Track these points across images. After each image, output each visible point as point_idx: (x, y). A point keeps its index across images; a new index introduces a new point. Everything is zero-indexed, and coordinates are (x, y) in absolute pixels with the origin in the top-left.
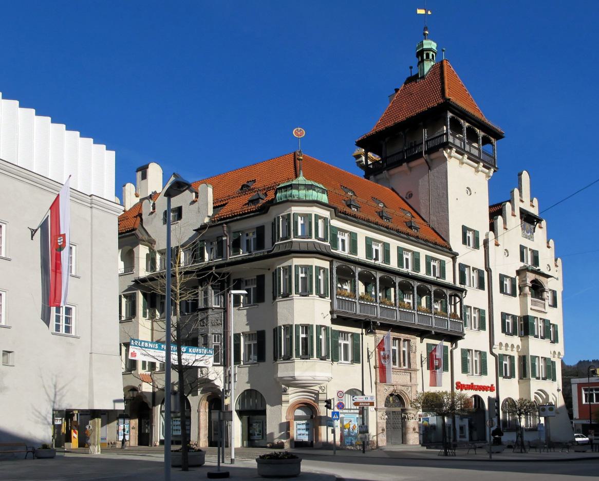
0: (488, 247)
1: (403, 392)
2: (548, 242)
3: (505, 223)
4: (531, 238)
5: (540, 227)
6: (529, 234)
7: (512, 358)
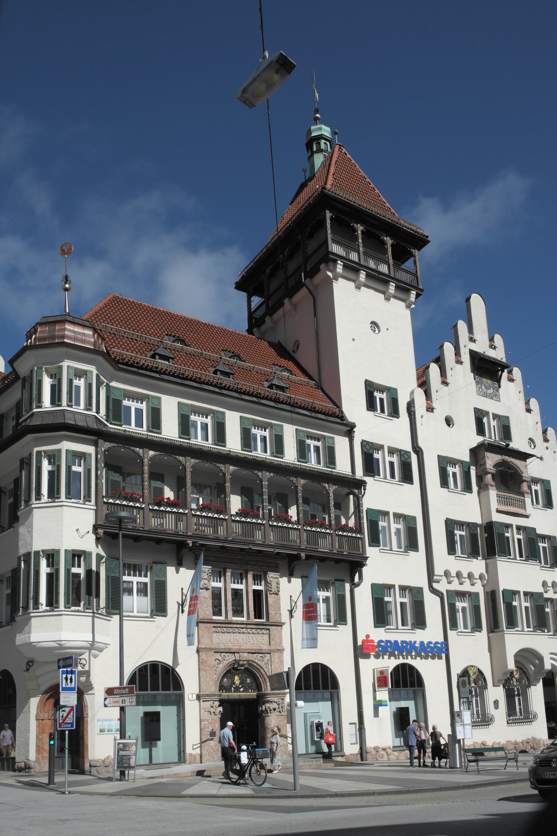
0: (414, 412)
1: (255, 664)
2: (527, 403)
3: (443, 373)
4: (495, 396)
5: (511, 380)
6: (491, 391)
7: (473, 596)
